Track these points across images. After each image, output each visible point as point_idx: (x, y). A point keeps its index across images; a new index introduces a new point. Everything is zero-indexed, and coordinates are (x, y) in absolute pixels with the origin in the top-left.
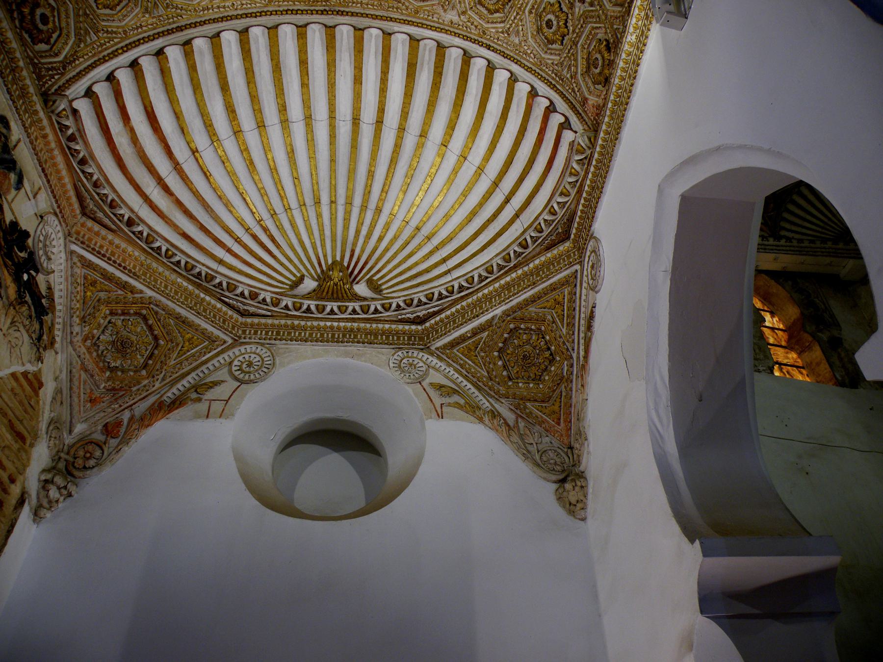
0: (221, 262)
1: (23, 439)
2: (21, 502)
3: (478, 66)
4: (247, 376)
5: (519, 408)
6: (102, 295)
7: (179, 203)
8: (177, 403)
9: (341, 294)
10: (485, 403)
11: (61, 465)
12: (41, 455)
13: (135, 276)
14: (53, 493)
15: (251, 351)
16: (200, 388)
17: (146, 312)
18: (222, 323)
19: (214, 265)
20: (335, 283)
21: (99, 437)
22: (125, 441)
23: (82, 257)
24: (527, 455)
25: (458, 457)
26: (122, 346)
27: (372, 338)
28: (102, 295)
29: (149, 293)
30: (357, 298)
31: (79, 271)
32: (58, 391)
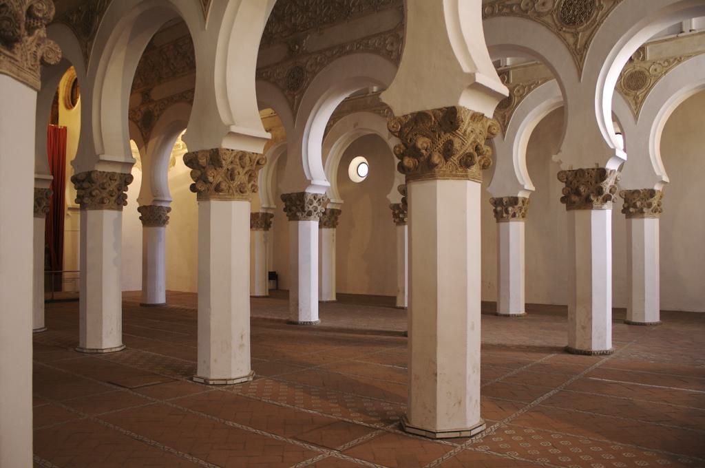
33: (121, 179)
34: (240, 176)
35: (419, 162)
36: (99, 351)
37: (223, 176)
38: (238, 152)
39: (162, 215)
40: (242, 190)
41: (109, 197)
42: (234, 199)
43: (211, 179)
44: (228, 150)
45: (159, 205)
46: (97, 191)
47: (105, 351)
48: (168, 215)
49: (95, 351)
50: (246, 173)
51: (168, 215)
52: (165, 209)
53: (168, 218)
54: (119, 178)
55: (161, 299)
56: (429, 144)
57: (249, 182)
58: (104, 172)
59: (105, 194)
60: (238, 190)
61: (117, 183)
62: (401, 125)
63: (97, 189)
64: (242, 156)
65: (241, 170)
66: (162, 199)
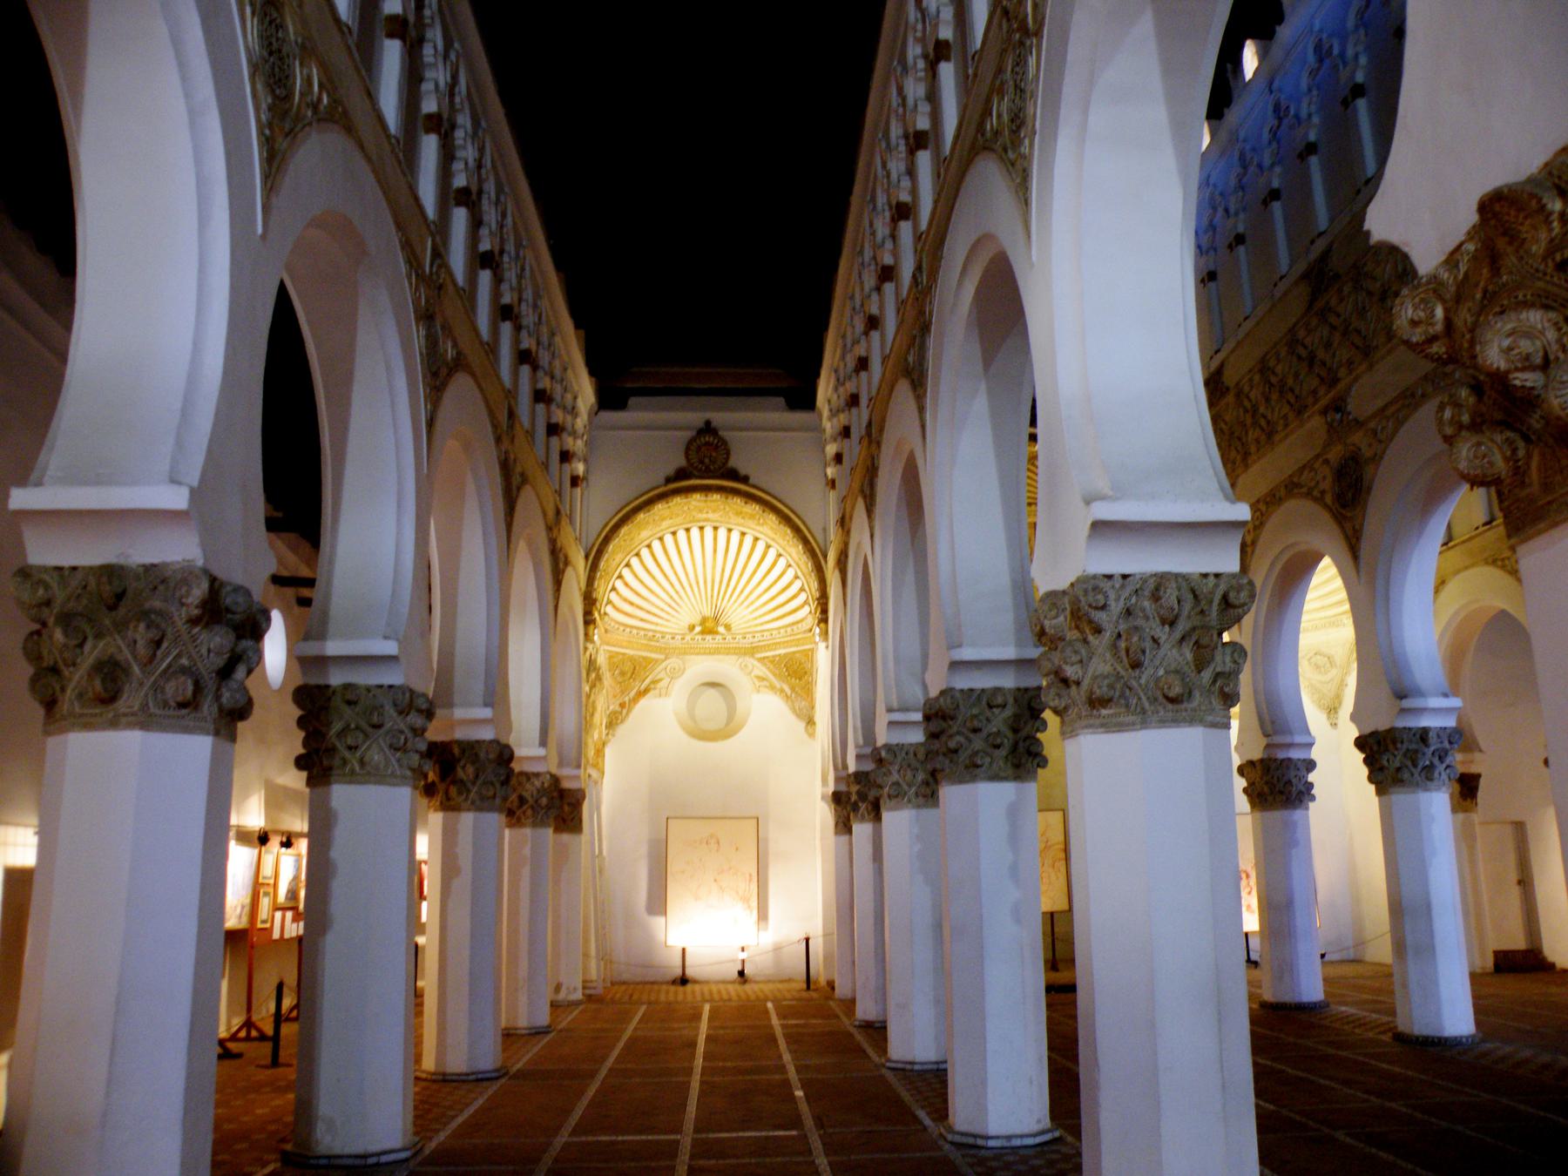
3: (772, 554)
4: (675, 675)
5: (793, 689)
8: (646, 691)
9: (712, 632)
10: (778, 684)
15: (673, 662)
16: (655, 682)
17: (631, 659)
18: (660, 650)
20: (709, 626)
24: (794, 710)
25: (766, 711)
26: (623, 674)
27: (728, 651)
30: (717, 633)
33: (1016, 700)
34: (1165, 648)
35: (1526, 439)
36: (980, 1142)
37: (1108, 655)
38: (1144, 579)
40: (1171, 695)
41: (989, 750)
42: (1144, 725)
43: (1070, 671)
44: (1109, 577)
45: (1281, 755)
46: (959, 738)
47: (991, 1143)
48: (1311, 777)
49: (971, 1141)
50: (1183, 638)
51: (1311, 777)
53: (1311, 785)
54: (1011, 701)
55: (1311, 989)
56: (1551, 335)
57: (1200, 666)
58: (971, 690)
59: (978, 743)
60: (1159, 695)
61: (1008, 712)
62: (1444, 301)
63: (958, 733)
64: (1157, 589)
65: (1162, 633)
66: (1288, 740)
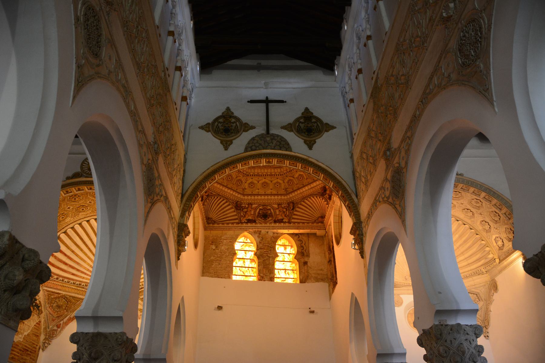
0: (83, 278)
1: (38, 336)
2: (39, 349)
6: (53, 297)
7: (71, 266)
11: (47, 337)
12: (42, 337)
13: (60, 290)
14: (46, 345)
17: (64, 297)
19: (81, 280)
21: (55, 328)
22: (62, 330)
23: (46, 290)
28: (53, 297)
29: (64, 293)
31: (46, 293)
32: (45, 321)
39: (466, 344)
45: (452, 322)
52: (468, 329)
